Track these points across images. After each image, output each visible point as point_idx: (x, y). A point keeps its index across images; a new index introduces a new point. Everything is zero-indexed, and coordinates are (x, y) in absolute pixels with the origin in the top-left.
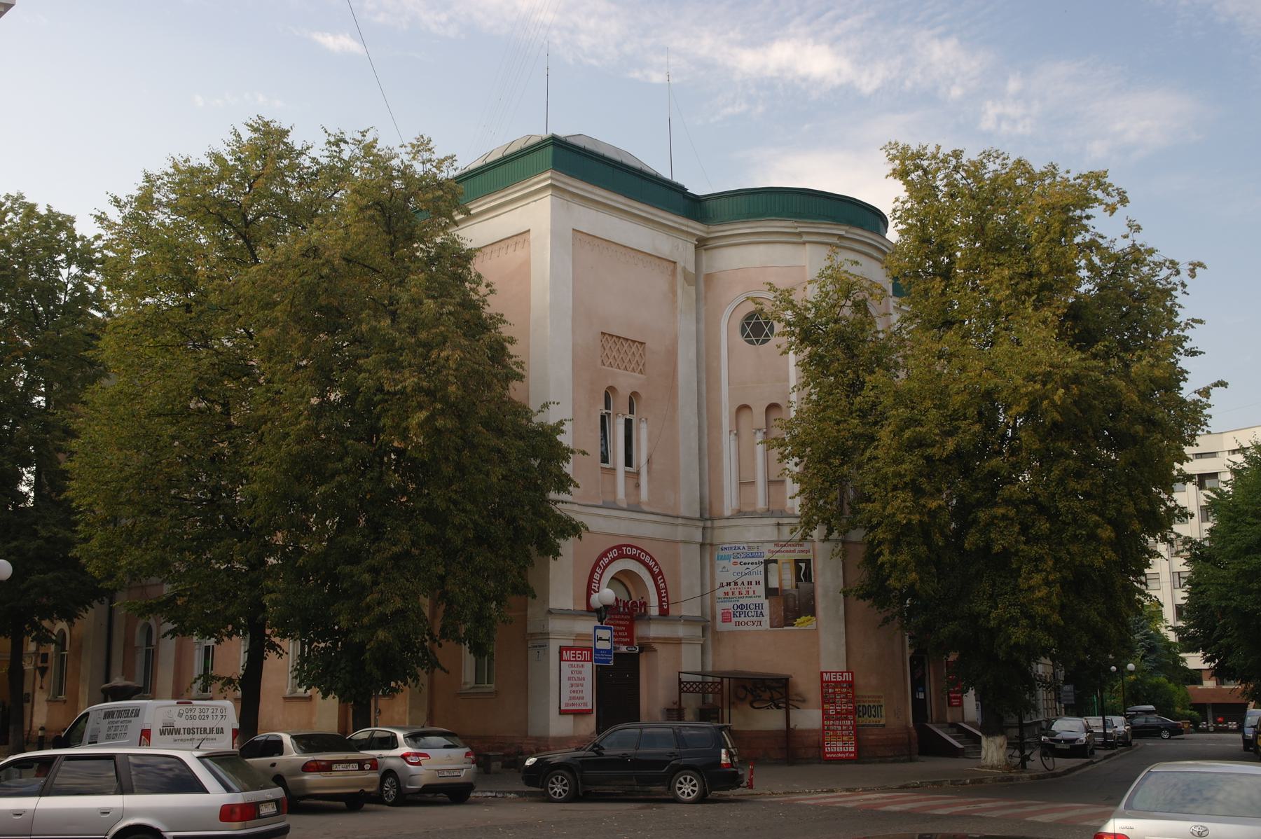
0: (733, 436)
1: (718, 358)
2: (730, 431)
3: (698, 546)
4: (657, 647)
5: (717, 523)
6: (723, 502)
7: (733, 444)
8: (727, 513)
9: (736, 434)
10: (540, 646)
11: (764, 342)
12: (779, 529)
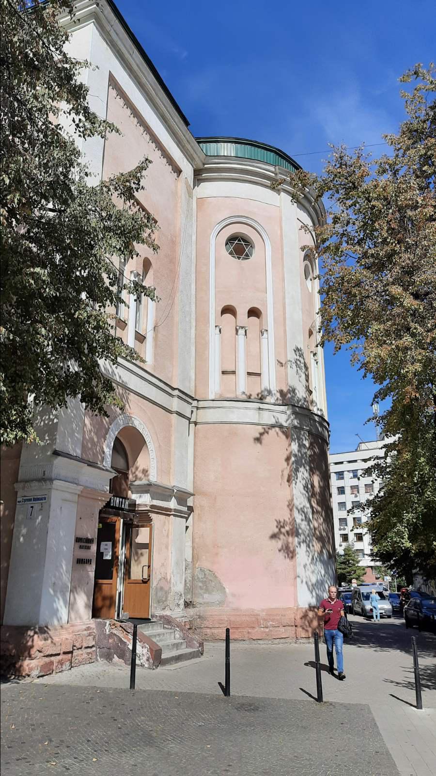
1: (207, 265)
2: (216, 326)
4: (153, 516)
5: (201, 404)
8: (212, 397)
9: (220, 331)
10: (35, 499)
11: (244, 259)
12: (259, 413)
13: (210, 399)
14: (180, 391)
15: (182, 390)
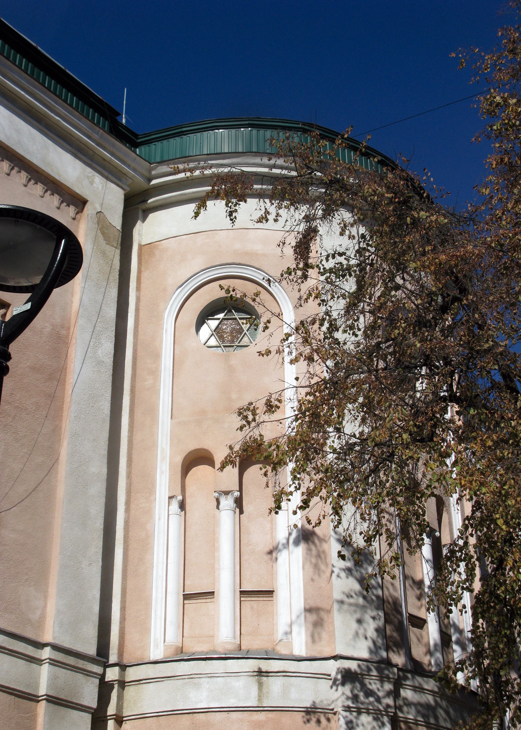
0: (175, 506)
2: (170, 498)
3: (87, 718)
5: (132, 674)
6: (148, 630)
7: (175, 522)
8: (156, 654)
9: (182, 506)
12: (260, 685)
13: (153, 658)
14: (56, 648)
15: (67, 644)
